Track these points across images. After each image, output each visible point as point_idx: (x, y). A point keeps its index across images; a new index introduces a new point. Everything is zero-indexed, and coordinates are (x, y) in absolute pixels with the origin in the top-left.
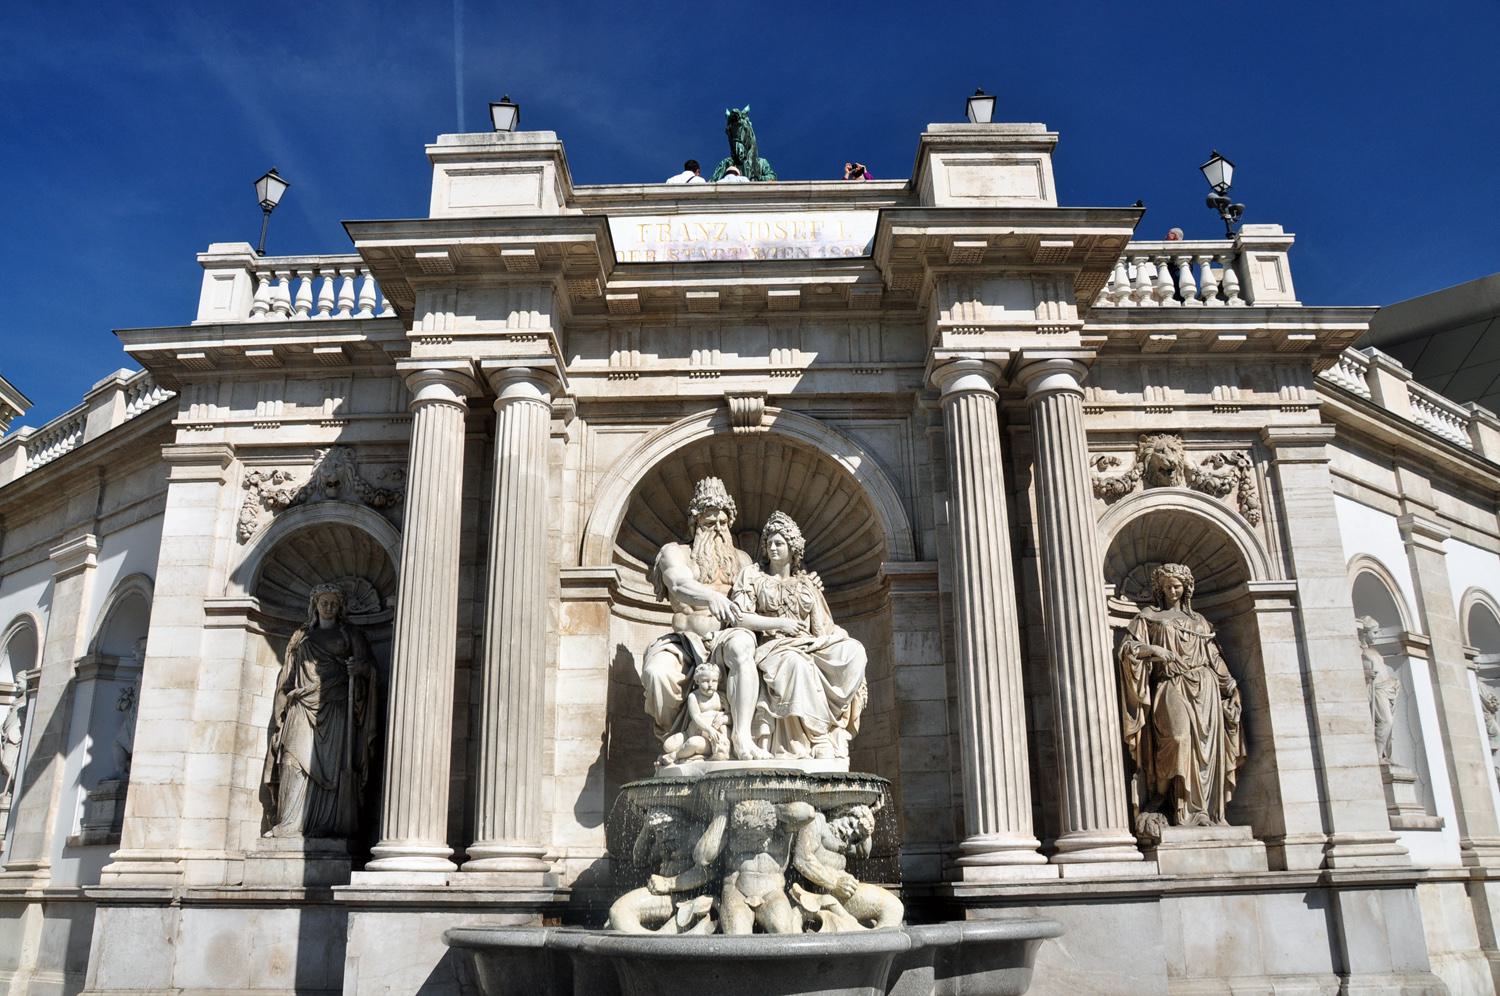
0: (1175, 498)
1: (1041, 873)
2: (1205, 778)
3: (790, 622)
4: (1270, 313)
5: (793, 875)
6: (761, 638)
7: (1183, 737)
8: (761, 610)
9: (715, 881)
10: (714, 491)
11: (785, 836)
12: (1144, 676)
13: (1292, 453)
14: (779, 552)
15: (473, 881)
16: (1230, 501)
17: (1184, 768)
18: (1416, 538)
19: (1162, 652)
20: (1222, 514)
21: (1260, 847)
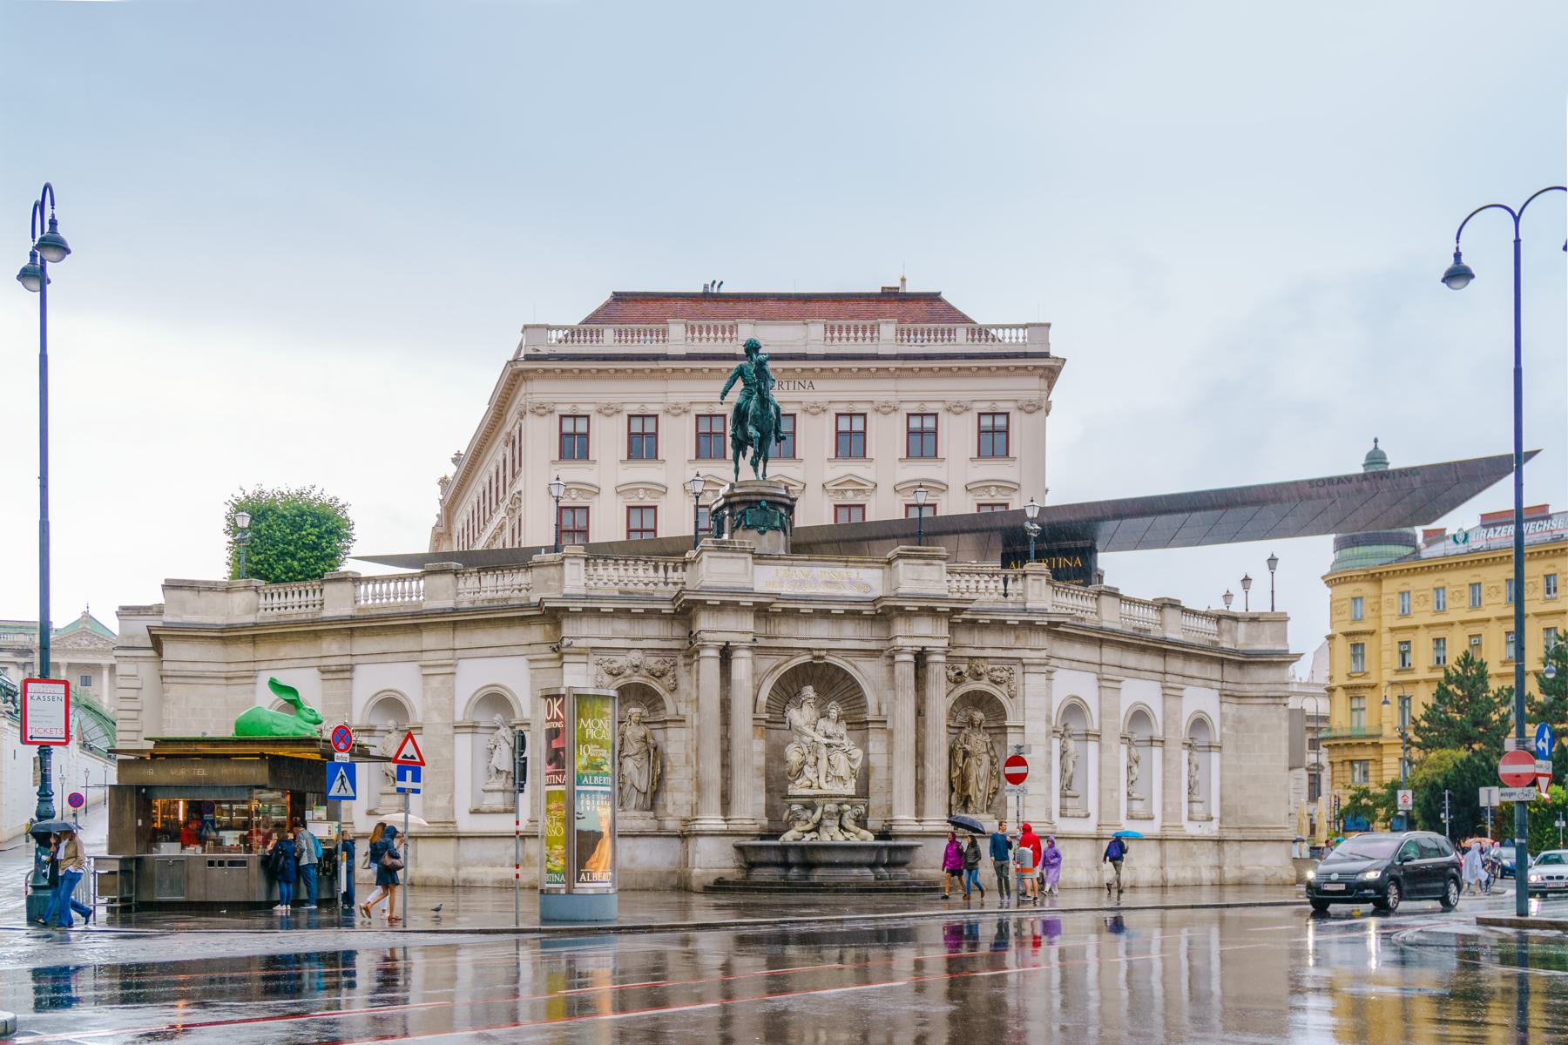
0: (983, 685)
1: (917, 828)
2: (979, 795)
3: (837, 741)
4: (1031, 612)
5: (841, 827)
6: (829, 746)
7: (972, 781)
8: (828, 737)
9: (816, 829)
10: (809, 691)
11: (840, 814)
12: (958, 756)
13: (1032, 669)
14: (834, 714)
15: (735, 826)
16: (1004, 688)
17: (971, 791)
18: (1104, 684)
19: (968, 747)
20: (999, 692)
21: (996, 823)
